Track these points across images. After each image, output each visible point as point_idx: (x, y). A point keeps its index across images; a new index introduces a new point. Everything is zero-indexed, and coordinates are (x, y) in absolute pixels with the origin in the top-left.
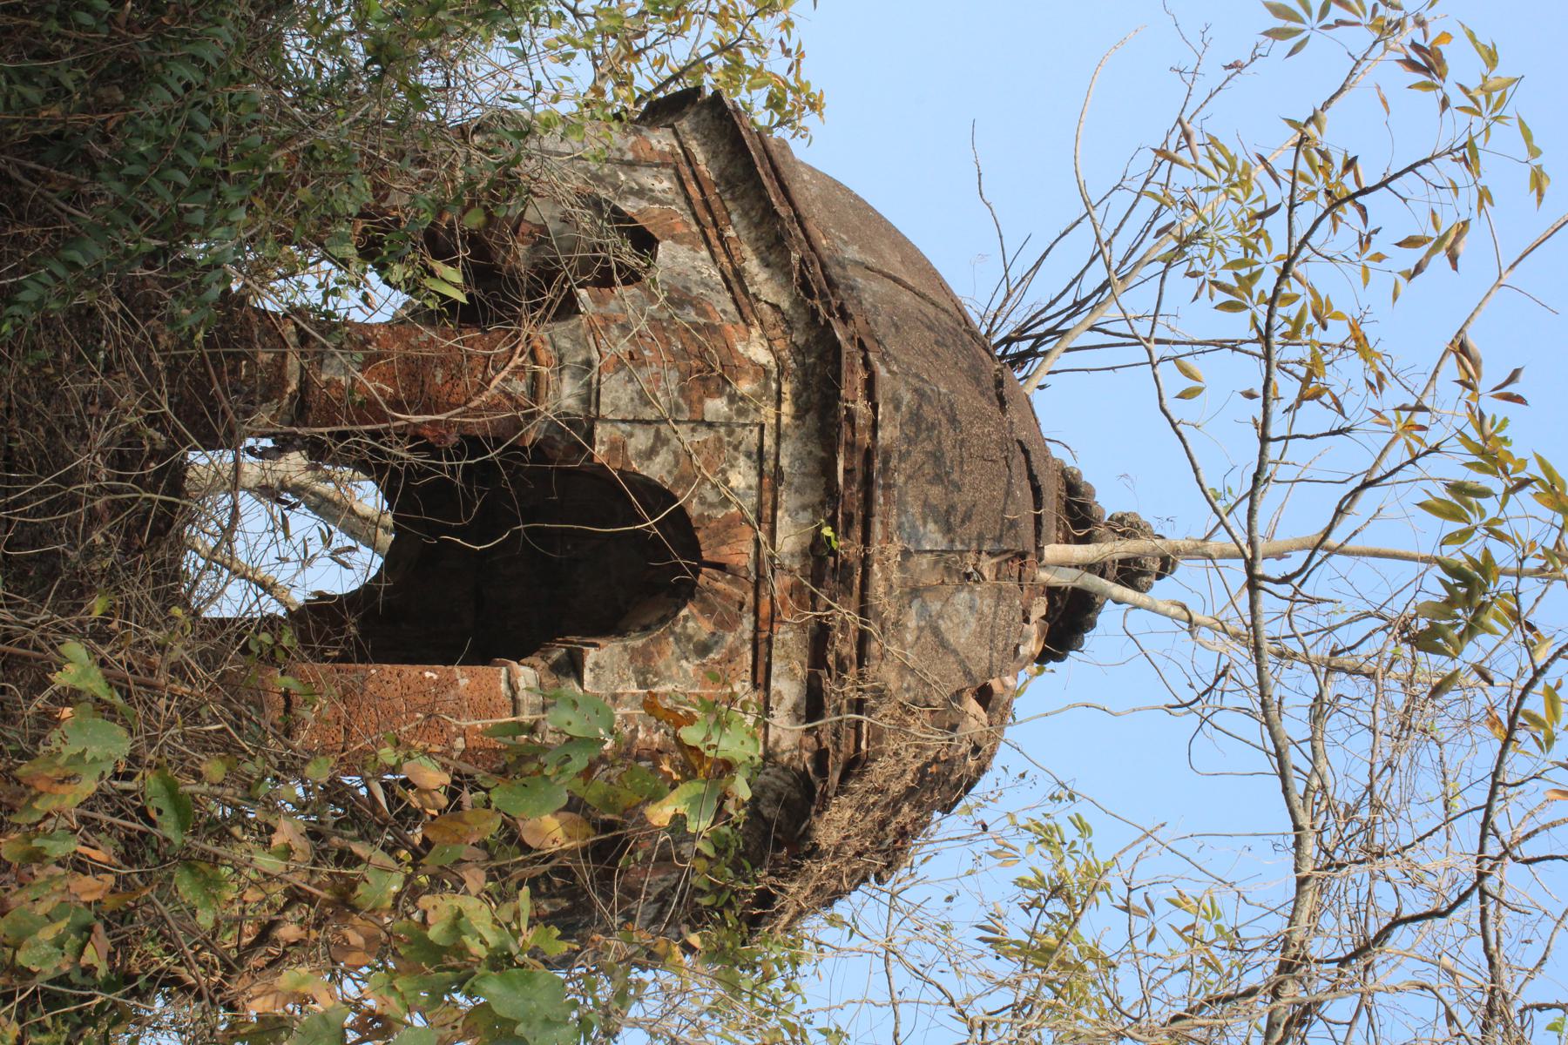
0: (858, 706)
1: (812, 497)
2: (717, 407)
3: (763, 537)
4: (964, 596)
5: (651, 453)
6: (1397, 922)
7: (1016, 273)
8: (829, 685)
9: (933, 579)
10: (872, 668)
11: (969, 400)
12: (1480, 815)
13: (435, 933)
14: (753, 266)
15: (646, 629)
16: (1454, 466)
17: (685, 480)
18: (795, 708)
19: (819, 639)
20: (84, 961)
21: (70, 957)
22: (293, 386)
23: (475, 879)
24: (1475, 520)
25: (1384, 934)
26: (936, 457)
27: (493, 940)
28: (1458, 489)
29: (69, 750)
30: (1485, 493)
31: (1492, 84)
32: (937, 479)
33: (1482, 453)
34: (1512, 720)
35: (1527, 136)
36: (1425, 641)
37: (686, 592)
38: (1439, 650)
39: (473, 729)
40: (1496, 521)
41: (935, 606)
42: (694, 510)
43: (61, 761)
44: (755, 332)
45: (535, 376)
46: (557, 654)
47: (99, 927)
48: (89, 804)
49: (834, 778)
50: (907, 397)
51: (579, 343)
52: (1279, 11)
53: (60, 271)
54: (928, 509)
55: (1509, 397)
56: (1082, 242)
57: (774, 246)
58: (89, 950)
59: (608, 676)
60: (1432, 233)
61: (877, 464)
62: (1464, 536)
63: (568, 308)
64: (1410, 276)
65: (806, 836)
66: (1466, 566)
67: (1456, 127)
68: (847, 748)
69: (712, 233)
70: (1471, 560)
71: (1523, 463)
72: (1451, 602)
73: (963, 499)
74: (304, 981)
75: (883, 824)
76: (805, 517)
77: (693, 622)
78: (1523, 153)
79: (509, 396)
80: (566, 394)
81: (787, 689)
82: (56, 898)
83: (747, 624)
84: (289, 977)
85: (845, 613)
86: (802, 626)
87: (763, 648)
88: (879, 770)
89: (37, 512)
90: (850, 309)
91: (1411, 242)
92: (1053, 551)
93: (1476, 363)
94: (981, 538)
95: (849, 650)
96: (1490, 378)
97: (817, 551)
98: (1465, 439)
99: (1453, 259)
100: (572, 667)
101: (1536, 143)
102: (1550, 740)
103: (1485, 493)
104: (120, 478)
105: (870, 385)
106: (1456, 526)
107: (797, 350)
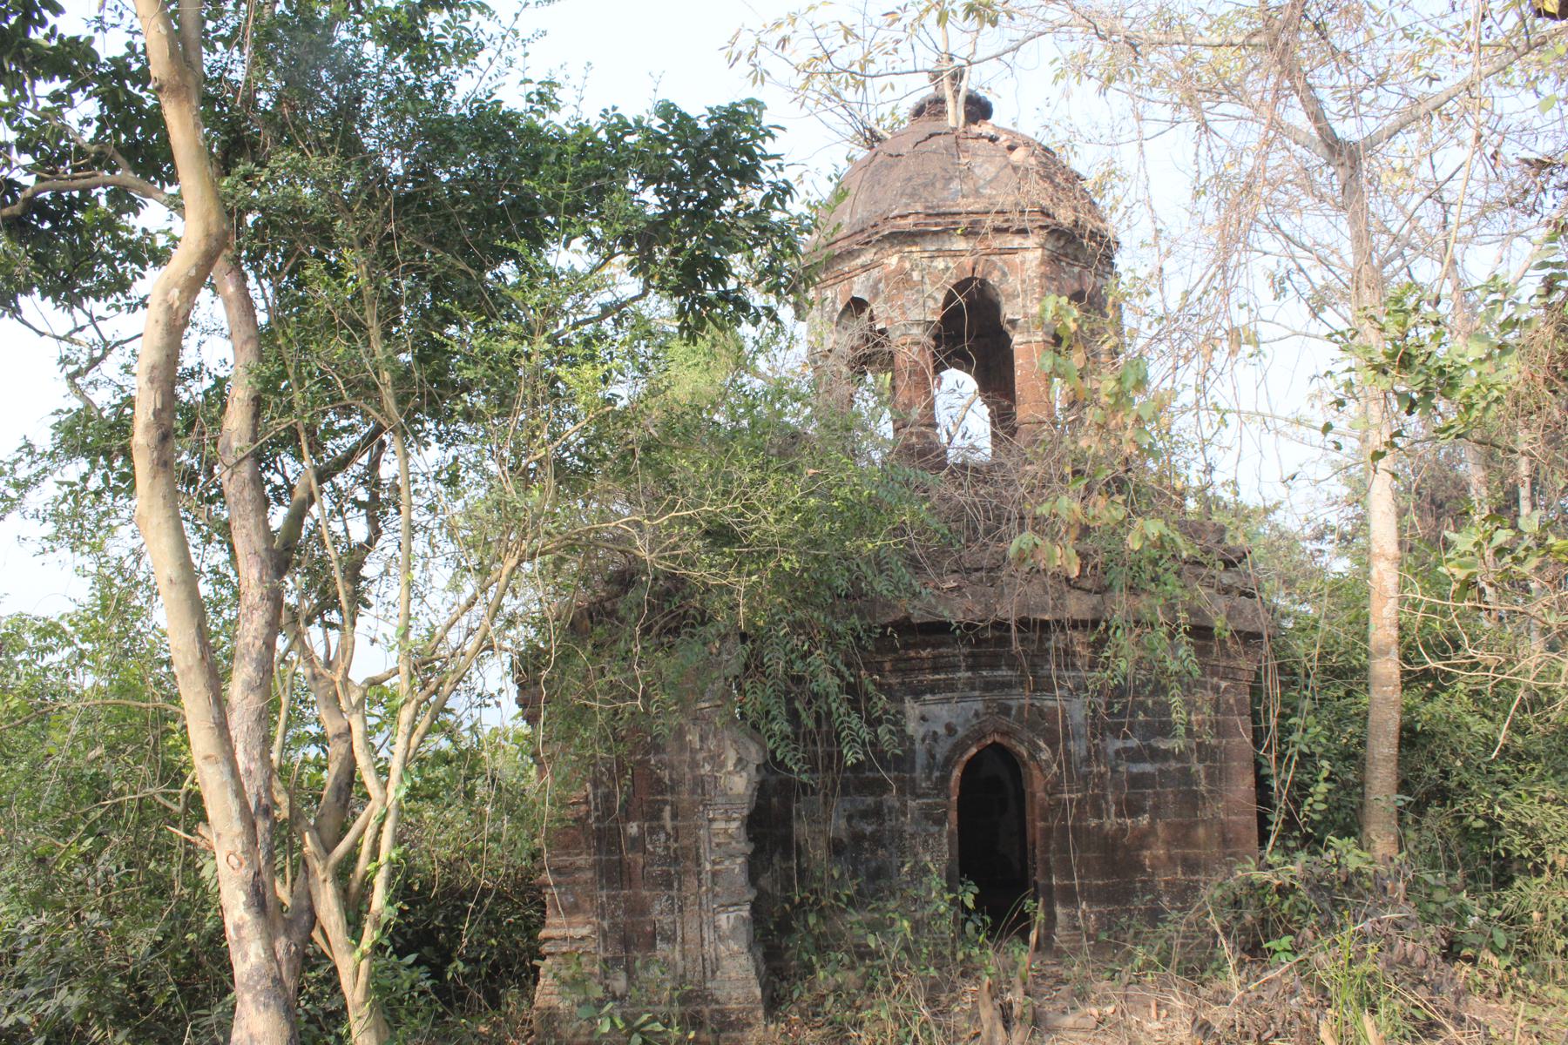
0: (1022, 212)
1: (946, 237)
2: (916, 276)
5: (935, 299)
7: (838, 138)
9: (971, 183)
10: (1007, 208)
11: (899, 172)
13: (1112, 401)
14: (859, 261)
19: (998, 230)
26: (925, 186)
32: (933, 184)
37: (983, 282)
42: (954, 281)
46: (1007, 327)
49: (1049, 221)
51: (897, 328)
54: (945, 187)
56: (827, 116)
57: (851, 254)
59: (1017, 309)
62: (954, 12)
63: (882, 332)
68: (1038, 216)
77: (994, 279)
80: (916, 331)
81: (1017, 241)
83: (993, 258)
85: (989, 222)
88: (1046, 203)
95: (1001, 218)
100: (1013, 323)
107: (892, 246)
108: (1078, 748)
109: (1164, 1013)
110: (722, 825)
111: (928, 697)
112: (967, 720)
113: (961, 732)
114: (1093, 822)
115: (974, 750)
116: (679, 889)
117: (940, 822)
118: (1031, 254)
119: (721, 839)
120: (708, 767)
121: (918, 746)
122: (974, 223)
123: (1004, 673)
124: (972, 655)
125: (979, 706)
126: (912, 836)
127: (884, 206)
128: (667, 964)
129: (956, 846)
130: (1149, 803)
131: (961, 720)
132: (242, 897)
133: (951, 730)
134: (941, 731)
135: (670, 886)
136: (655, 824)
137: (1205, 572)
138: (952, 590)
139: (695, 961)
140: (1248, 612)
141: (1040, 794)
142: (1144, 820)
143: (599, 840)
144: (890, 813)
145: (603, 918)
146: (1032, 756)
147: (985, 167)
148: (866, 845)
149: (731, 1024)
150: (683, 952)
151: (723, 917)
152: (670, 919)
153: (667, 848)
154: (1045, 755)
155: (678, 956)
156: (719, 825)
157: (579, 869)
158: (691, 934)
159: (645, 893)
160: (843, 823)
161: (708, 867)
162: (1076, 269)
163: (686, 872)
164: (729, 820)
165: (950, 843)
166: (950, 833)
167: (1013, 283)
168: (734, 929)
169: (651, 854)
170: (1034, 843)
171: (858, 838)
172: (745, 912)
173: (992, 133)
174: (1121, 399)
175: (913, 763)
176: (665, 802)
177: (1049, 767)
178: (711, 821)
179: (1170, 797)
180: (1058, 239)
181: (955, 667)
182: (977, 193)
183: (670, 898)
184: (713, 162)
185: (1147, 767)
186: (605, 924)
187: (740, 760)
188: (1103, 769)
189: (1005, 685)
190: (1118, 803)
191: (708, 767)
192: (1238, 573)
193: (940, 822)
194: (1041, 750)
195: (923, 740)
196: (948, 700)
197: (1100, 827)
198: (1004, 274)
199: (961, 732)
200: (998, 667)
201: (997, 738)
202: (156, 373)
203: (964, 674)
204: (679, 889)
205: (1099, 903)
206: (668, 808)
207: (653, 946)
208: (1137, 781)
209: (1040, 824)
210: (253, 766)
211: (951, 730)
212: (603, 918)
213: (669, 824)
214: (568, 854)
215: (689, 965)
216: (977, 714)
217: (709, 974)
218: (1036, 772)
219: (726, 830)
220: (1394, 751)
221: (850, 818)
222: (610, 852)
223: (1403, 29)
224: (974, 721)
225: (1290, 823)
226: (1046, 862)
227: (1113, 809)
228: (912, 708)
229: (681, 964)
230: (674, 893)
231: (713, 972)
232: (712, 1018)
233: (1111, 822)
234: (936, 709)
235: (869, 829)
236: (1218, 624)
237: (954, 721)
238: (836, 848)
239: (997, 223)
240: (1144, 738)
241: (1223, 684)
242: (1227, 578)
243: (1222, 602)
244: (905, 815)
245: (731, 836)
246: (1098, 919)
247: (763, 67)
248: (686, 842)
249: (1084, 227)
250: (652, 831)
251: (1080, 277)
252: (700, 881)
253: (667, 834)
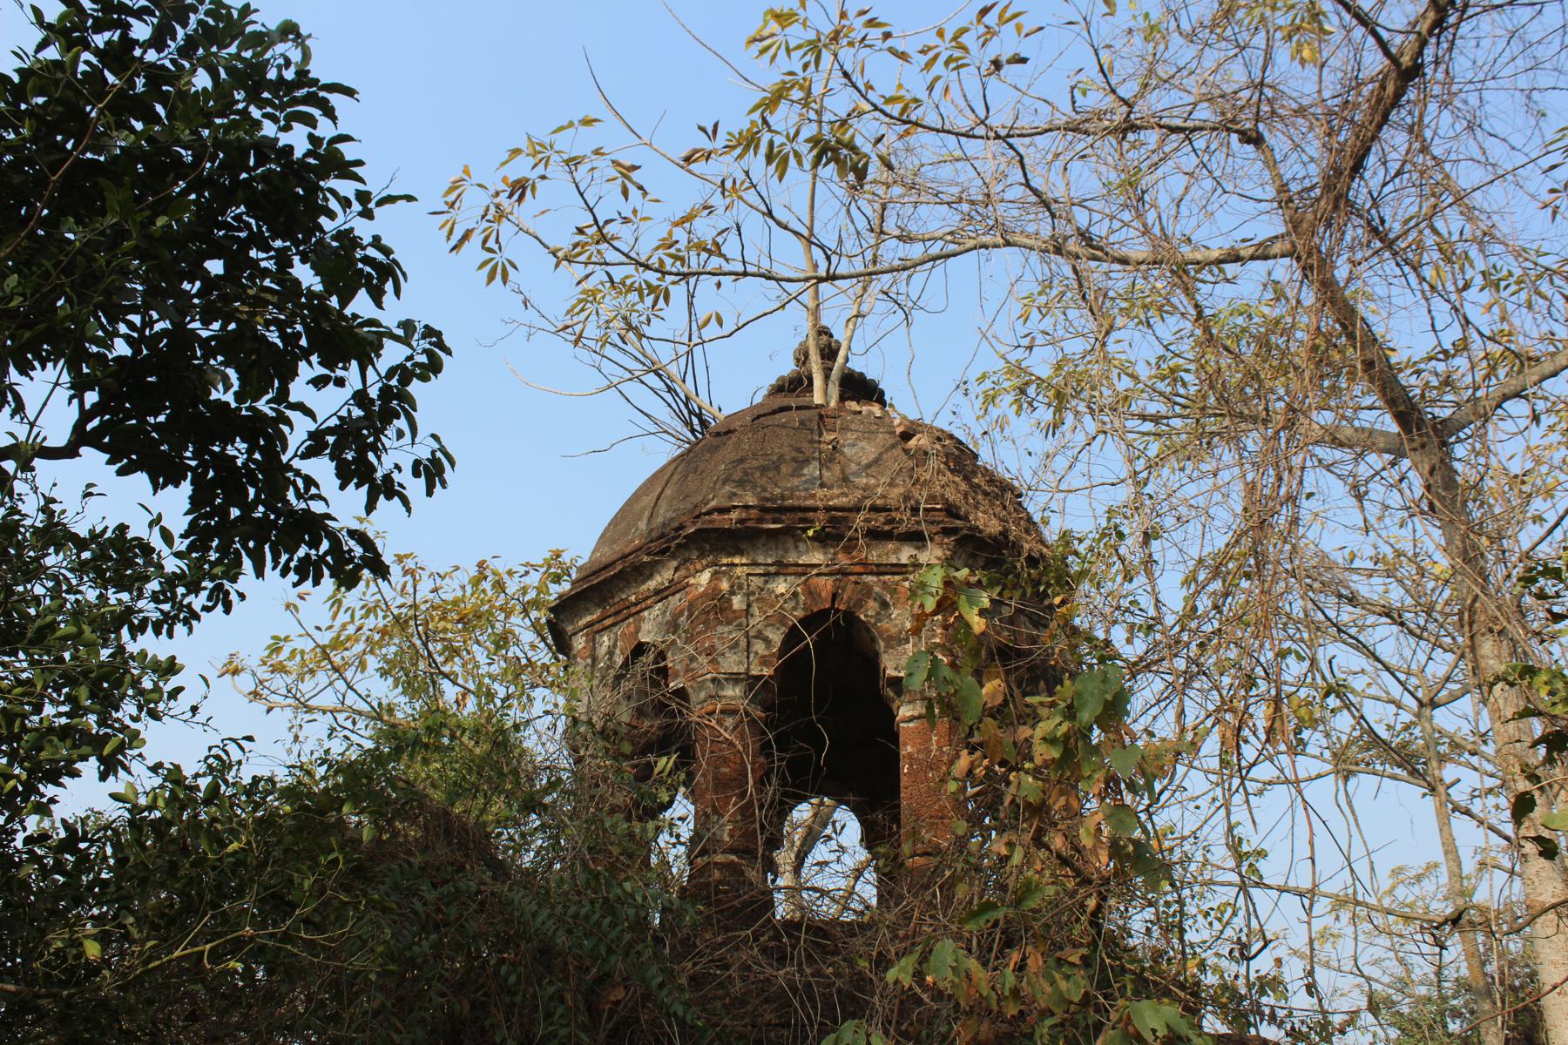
0: (915, 510)
2: (737, 602)
3: (815, 571)
5: (767, 641)
6: (1028, 185)
7: (653, 428)
8: (903, 529)
10: (892, 503)
11: (728, 452)
12: (962, 139)
14: (652, 584)
15: (874, 640)
16: (757, 163)
17: (782, 620)
18: (918, 548)
19: (876, 535)
20: (1078, 962)
21: (1076, 971)
22: (733, 857)
23: (1024, 732)
24: (787, 149)
25: (1035, 192)
27: (1058, 719)
28: (770, 158)
29: (950, 975)
30: (771, 143)
31: (530, 151)
32: (777, 469)
33: (748, 147)
34: (905, 122)
35: (561, 129)
36: (861, 174)
37: (850, 616)
38: (866, 166)
39: (938, 742)
40: (787, 136)
41: (853, 467)
42: (800, 613)
43: (956, 980)
44: (692, 581)
45: (722, 712)
47: (1058, 954)
48: (985, 964)
49: (959, 523)
51: (702, 686)
52: (491, 277)
53: (665, 992)
54: (796, 473)
55: (715, 131)
56: (632, 389)
57: (640, 572)
58: (1071, 959)
60: (619, 181)
61: (769, 504)
62: (798, 156)
63: (681, 694)
64: (645, 193)
65: (994, 538)
66: (815, 152)
67: (557, 170)
68: (940, 516)
69: (633, 610)
70: (811, 150)
71: (753, 123)
72: (837, 161)
73: (789, 454)
74: (1087, 831)
75: (986, 494)
76: (802, 547)
78: (572, 130)
79: (735, 728)
80: (733, 692)
81: (905, 555)
82: (1041, 980)
83: (870, 579)
84: (1086, 841)
86: (868, 546)
87: (882, 569)
88: (952, 495)
89: (814, 1008)
90: (676, 524)
91: (625, 193)
92: (818, 399)
93: (696, 151)
94: (812, 442)
95: (882, 517)
96: (703, 143)
97: (822, 539)
98: (741, 156)
99: (634, 168)
100: (896, 683)
101: (565, 123)
102: (916, 100)
103: (771, 143)
104: (792, 959)
105: (722, 511)
106: (792, 161)
107: (702, 555)
147: (857, 450)
174: (1072, 750)
184: (159, 109)
198: (884, 605)
223: (1483, 273)
247: (508, 253)
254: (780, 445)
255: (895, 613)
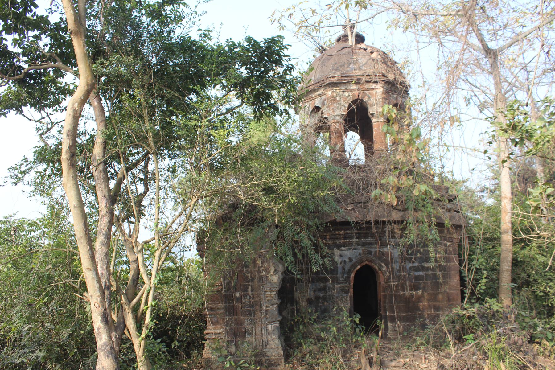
0: (376, 75)
1: (348, 84)
2: (338, 98)
4: (359, 61)
5: (345, 106)
7: (310, 49)
9: (357, 65)
10: (370, 74)
11: (332, 61)
14: (318, 93)
19: (367, 82)
26: (341, 66)
37: (362, 100)
42: (351, 100)
46: (370, 116)
49: (385, 78)
50: (334, 71)
51: (331, 117)
52: (280, 29)
54: (348, 67)
56: (307, 42)
57: (315, 91)
62: (351, 4)
63: (326, 118)
68: (381, 77)
77: (365, 99)
80: (338, 118)
81: (374, 86)
83: (366, 92)
88: (384, 72)
95: (368, 77)
97: (356, 83)
100: (372, 115)
105: (333, 77)
107: (329, 87)
108: (396, 266)
109: (427, 361)
110: (269, 293)
111: (342, 248)
112: (357, 256)
113: (354, 260)
114: (402, 293)
115: (359, 267)
116: (254, 316)
117: (347, 292)
118: (379, 90)
119: (269, 298)
120: (264, 273)
121: (339, 265)
122: (358, 79)
123: (370, 239)
124: (358, 233)
125: (361, 251)
126: (337, 297)
127: (327, 74)
128: (250, 343)
129: (353, 301)
130: (422, 286)
131: (354, 256)
132: (100, 318)
133: (350, 259)
134: (347, 260)
135: (251, 315)
136: (245, 293)
137: (441, 203)
138: (351, 210)
139: (260, 342)
140: (457, 218)
141: (383, 283)
142: (420, 292)
143: (226, 298)
144: (329, 289)
145: (227, 326)
146: (380, 269)
147: (362, 59)
148: (320, 300)
149: (272, 364)
150: (255, 338)
151: (270, 326)
152: (251, 326)
153: (250, 301)
154: (384, 269)
155: (254, 340)
156: (268, 293)
157: (218, 309)
158: (258, 332)
159: (242, 317)
160: (312, 293)
161: (264, 308)
162: (395, 96)
163: (257, 310)
164: (272, 291)
165: (350, 300)
166: (350, 297)
167: (372, 100)
168: (274, 330)
169: (245, 303)
170: (380, 300)
171: (317, 298)
172: (277, 324)
173: (365, 47)
174: (411, 142)
175: (337, 271)
176: (249, 285)
177: (386, 273)
178: (265, 292)
179: (429, 284)
180: (389, 85)
181: (352, 238)
182: (359, 68)
183: (251, 319)
184: (266, 58)
185: (421, 273)
186: (228, 328)
187: (275, 270)
188: (405, 274)
189: (370, 244)
190: (410, 286)
191: (264, 273)
192: (453, 204)
193: (347, 292)
194: (383, 267)
195: (341, 263)
196: (350, 249)
197: (404, 294)
199: (354, 260)
200: (368, 238)
201: (367, 263)
202: (70, 133)
203: (355, 240)
204: (254, 316)
205: (404, 321)
206: (250, 287)
207: (245, 336)
208: (417, 278)
209: (382, 293)
210: (104, 272)
211: (350, 259)
212: (227, 326)
213: (250, 293)
214: (215, 304)
215: (258, 343)
216: (360, 254)
217: (265, 346)
218: (381, 275)
219: (271, 295)
220: (510, 268)
221: (315, 291)
222: (229, 303)
224: (359, 257)
225: (472, 293)
226: (385, 307)
227: (409, 288)
228: (337, 252)
229: (255, 343)
230: (252, 317)
231: (266, 346)
232: (266, 362)
233: (408, 293)
234: (345, 252)
235: (321, 295)
236: (446, 222)
237: (352, 256)
238: (310, 302)
239: (367, 79)
240: (420, 263)
241: (448, 244)
242: (449, 206)
243: (448, 214)
244: (334, 290)
245: (272, 297)
246: (403, 327)
247: (284, 24)
248: (256, 299)
249: (398, 81)
250: (244, 295)
251: (396, 98)
252: (261, 313)
253: (250, 296)
254: (344, 59)
255: (372, 99)
